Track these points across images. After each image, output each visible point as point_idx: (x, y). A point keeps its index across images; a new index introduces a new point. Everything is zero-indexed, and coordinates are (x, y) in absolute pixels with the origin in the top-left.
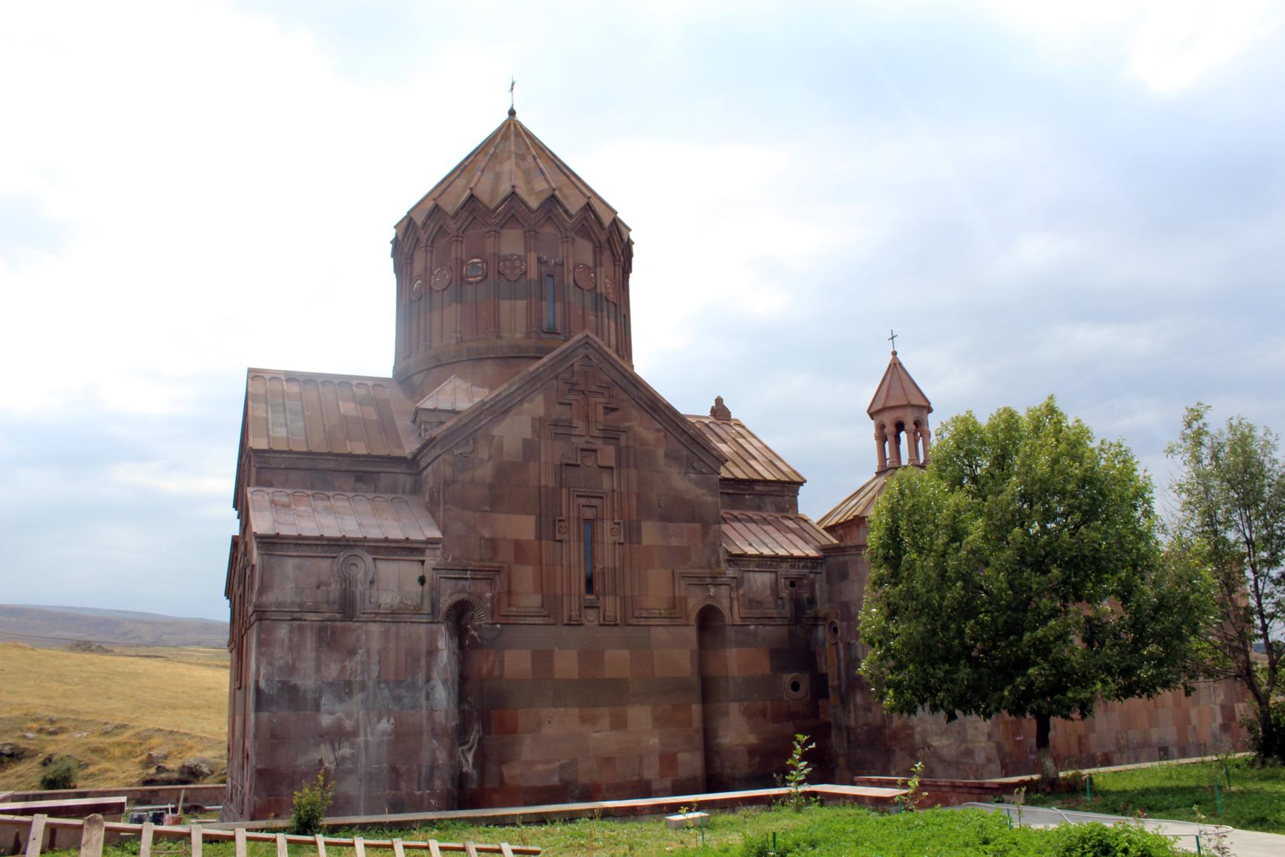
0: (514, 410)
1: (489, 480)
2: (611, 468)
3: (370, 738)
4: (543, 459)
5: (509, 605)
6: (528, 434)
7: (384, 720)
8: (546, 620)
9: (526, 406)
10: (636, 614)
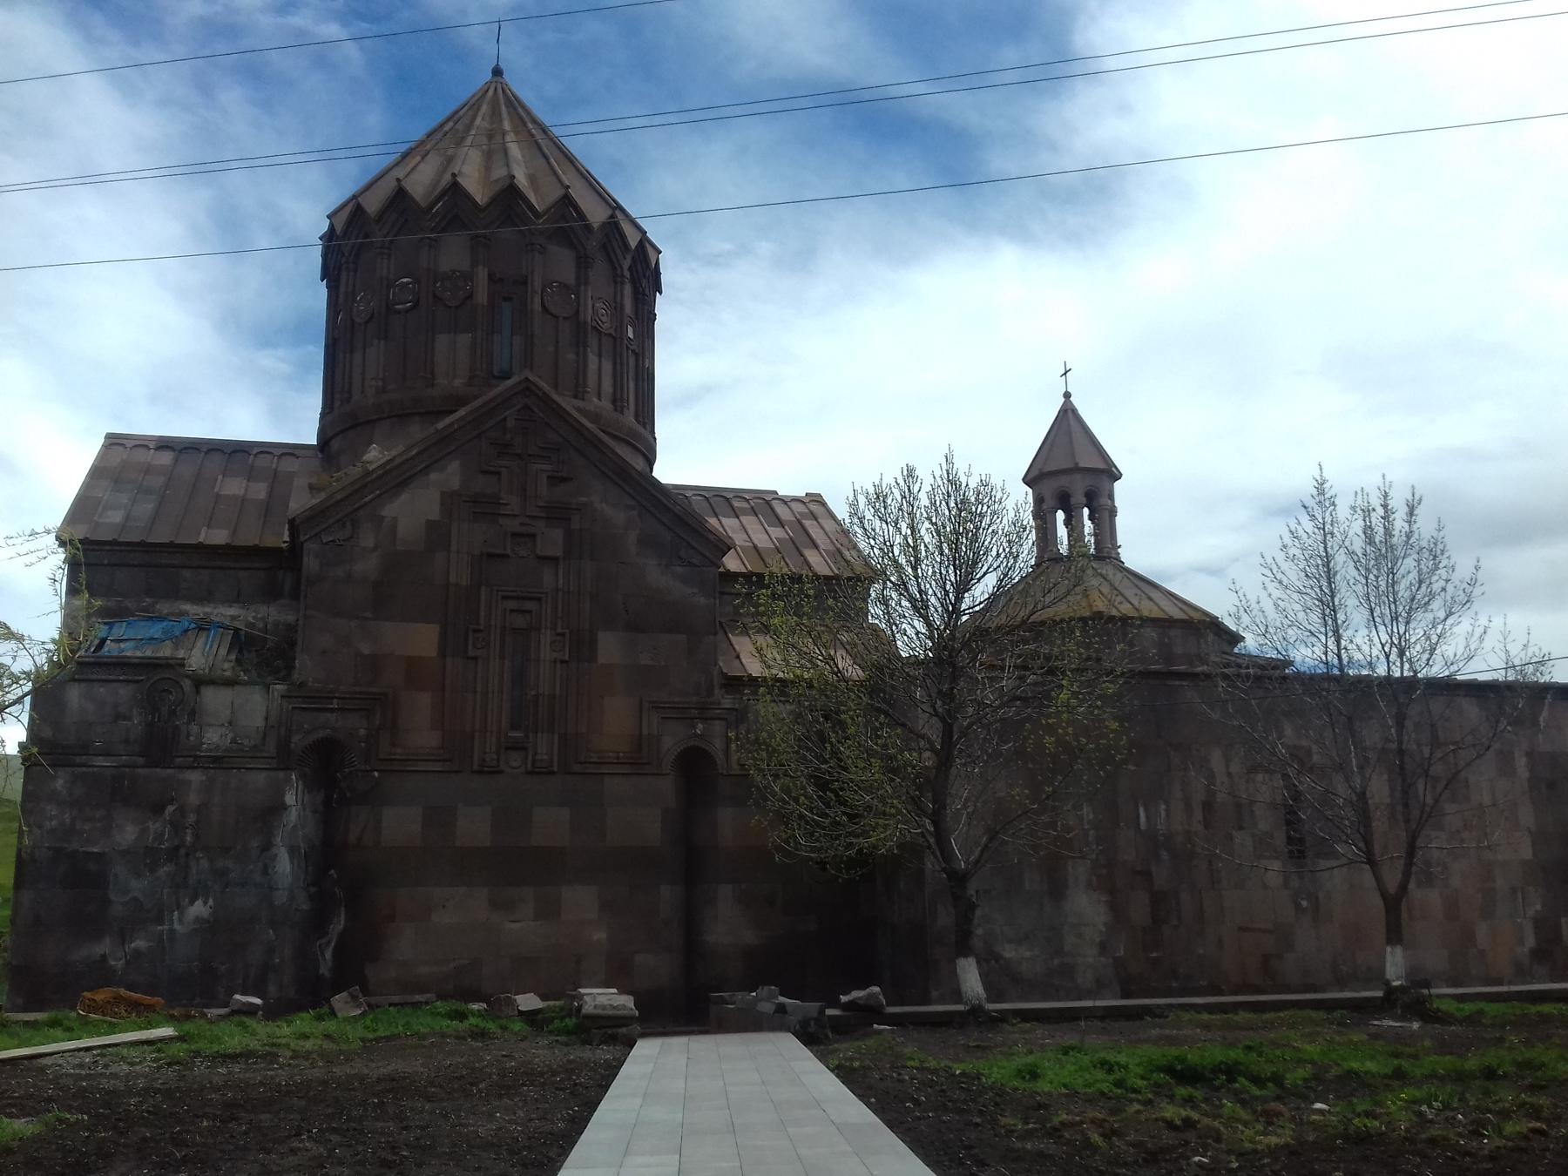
2: (555, 559)
3: (177, 926)
4: (454, 547)
6: (434, 512)
7: (199, 903)
9: (434, 476)
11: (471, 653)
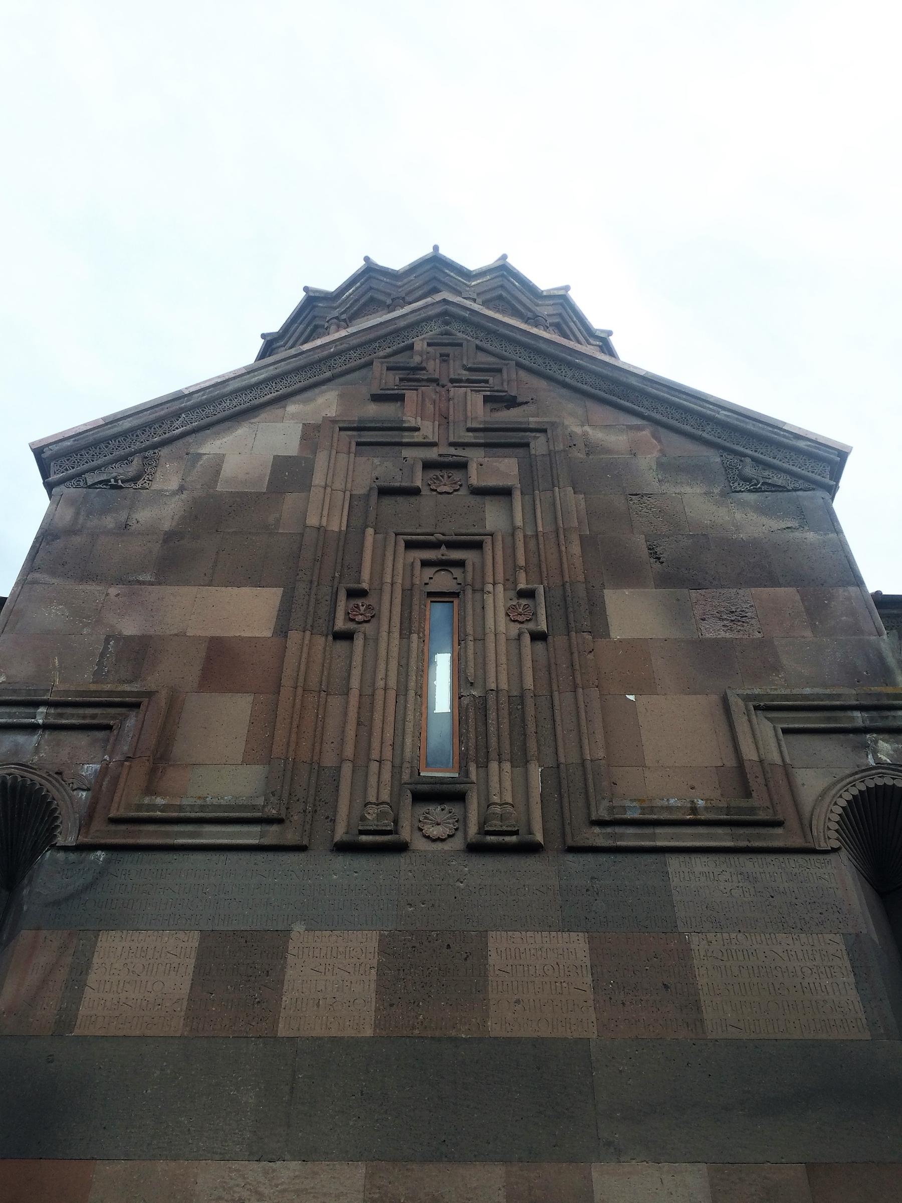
0: (264, 415)
1: (167, 526)
5: (150, 790)
8: (273, 835)
9: (292, 408)
10: (605, 815)
11: (340, 624)
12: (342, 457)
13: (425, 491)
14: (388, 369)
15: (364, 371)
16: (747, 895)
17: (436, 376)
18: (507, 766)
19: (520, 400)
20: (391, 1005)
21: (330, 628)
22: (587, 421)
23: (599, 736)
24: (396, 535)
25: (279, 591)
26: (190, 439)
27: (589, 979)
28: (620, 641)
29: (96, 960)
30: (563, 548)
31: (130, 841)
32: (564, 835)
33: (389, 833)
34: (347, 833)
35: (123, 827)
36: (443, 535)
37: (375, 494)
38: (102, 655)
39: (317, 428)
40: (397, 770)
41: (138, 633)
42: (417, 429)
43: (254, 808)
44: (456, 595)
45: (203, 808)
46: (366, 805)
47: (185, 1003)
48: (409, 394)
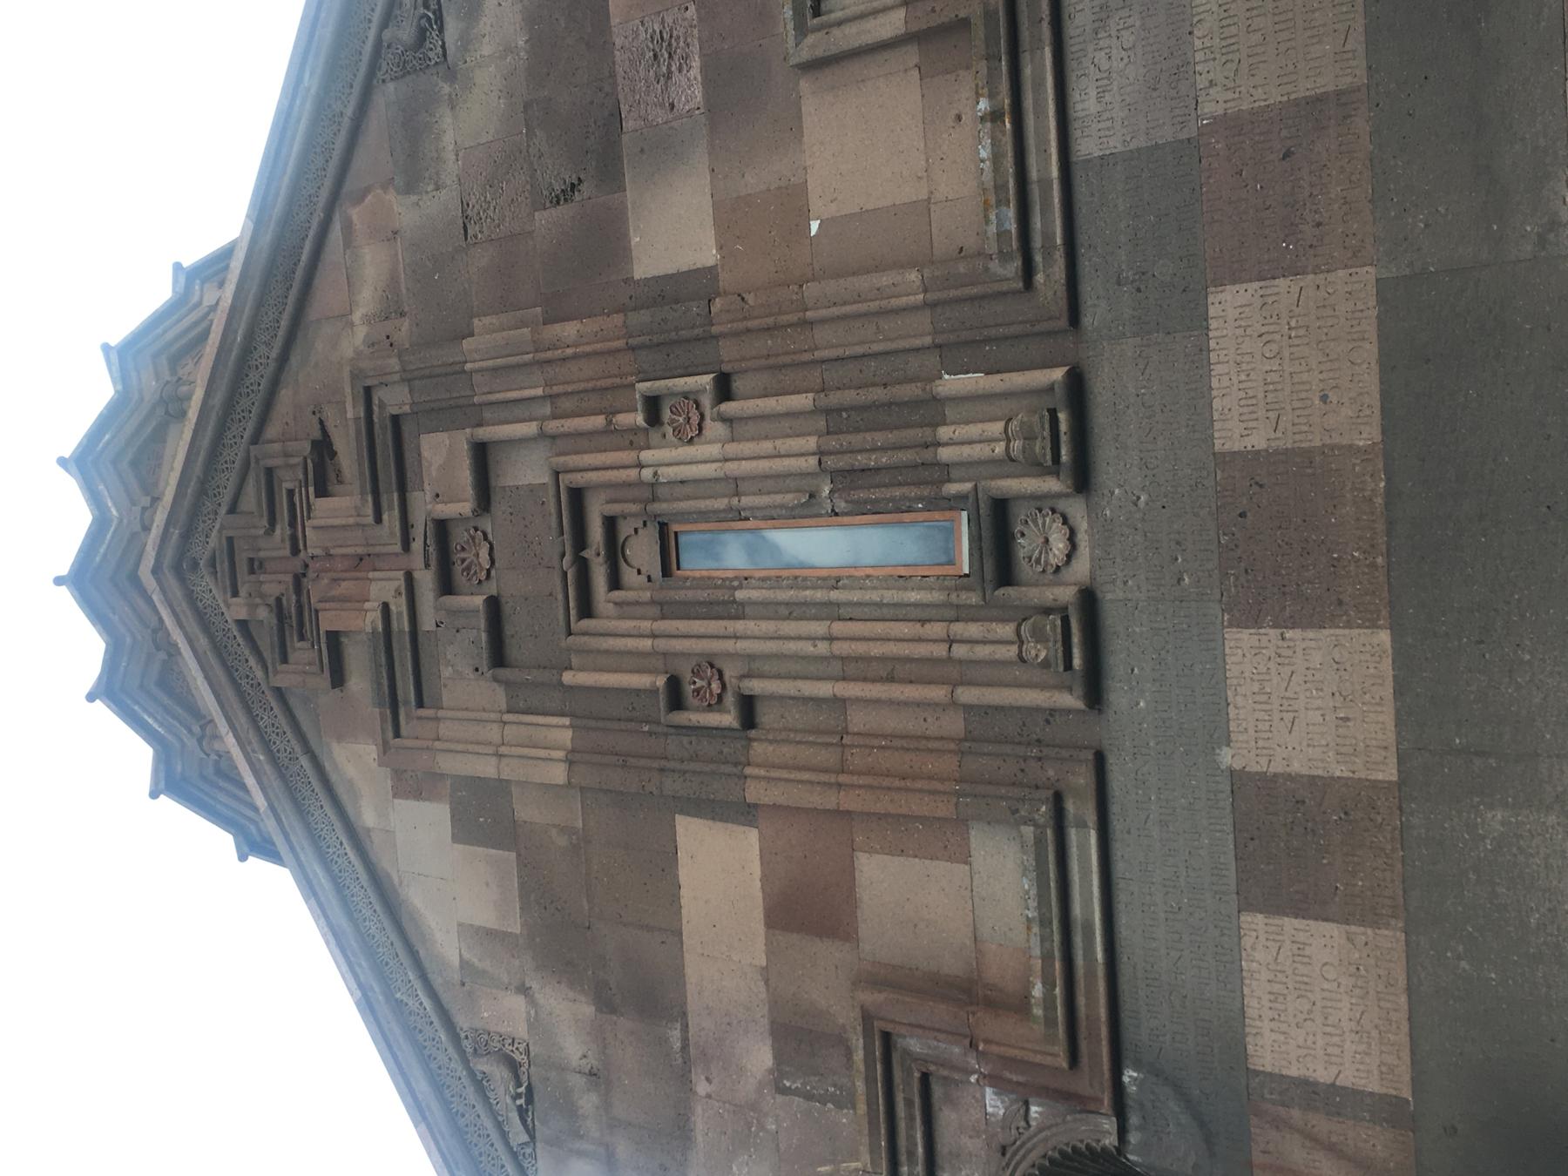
0: (384, 863)
1: (588, 1010)
5: (1021, 1006)
8: (1080, 809)
9: (368, 817)
11: (728, 718)
12: (445, 729)
13: (492, 588)
14: (285, 660)
15: (293, 702)
16: (1130, 21)
17: (289, 578)
18: (944, 432)
19: (317, 434)
20: (1340, 603)
21: (738, 734)
22: (345, 317)
23: (885, 280)
24: (570, 634)
25: (681, 820)
26: (437, 982)
27: (1282, 283)
28: (720, 248)
29: (1293, 1072)
30: (569, 351)
31: (1104, 1031)
32: (1049, 333)
33: (1066, 622)
34: (1070, 690)
35: (1083, 1046)
36: (563, 555)
37: (504, 673)
38: (809, 1097)
39: (398, 775)
40: (961, 614)
41: (769, 1042)
42: (386, 607)
43: (1039, 842)
44: (663, 528)
45: (1044, 922)
46: (1023, 660)
47: (1353, 928)
48: (325, 626)
